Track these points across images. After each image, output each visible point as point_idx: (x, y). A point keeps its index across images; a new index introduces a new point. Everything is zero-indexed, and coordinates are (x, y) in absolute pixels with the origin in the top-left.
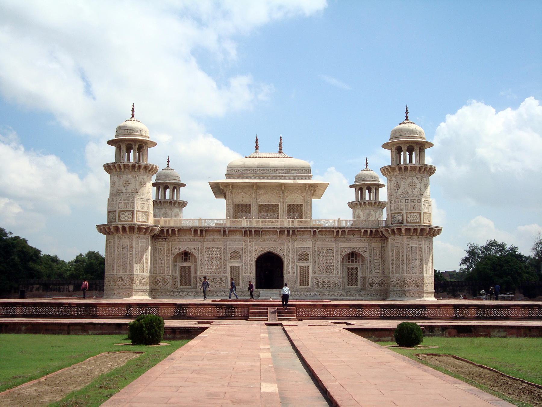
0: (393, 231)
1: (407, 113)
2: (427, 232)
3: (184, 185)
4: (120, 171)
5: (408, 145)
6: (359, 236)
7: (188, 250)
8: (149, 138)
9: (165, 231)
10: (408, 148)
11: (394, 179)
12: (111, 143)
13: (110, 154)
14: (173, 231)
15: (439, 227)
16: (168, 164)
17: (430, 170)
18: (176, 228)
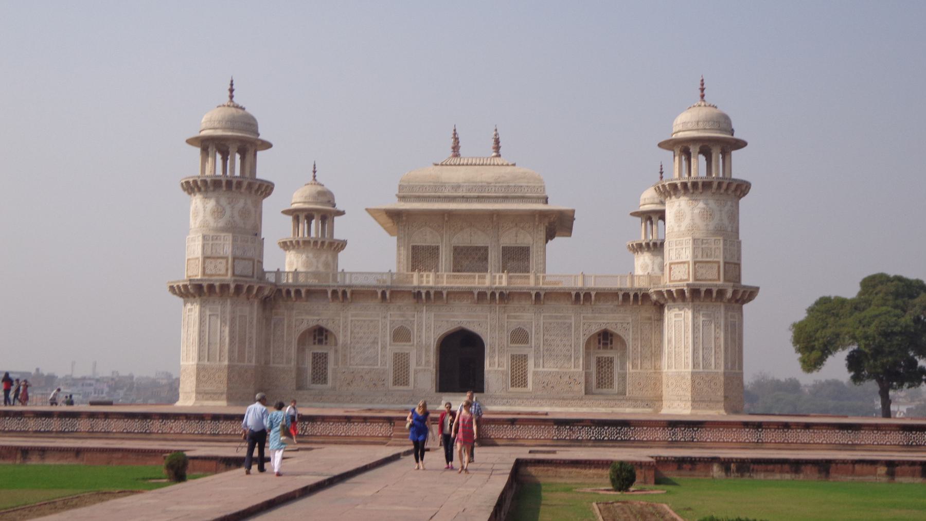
0: (669, 292)
1: (702, 90)
2: (729, 294)
3: (341, 213)
4: (206, 191)
5: (701, 144)
6: (616, 303)
7: (323, 324)
8: (258, 135)
9: (284, 291)
10: (701, 148)
11: (677, 204)
12: (192, 142)
13: (192, 164)
14: (298, 292)
15: (751, 287)
16: (315, 176)
17: (742, 188)
18: (303, 286)
